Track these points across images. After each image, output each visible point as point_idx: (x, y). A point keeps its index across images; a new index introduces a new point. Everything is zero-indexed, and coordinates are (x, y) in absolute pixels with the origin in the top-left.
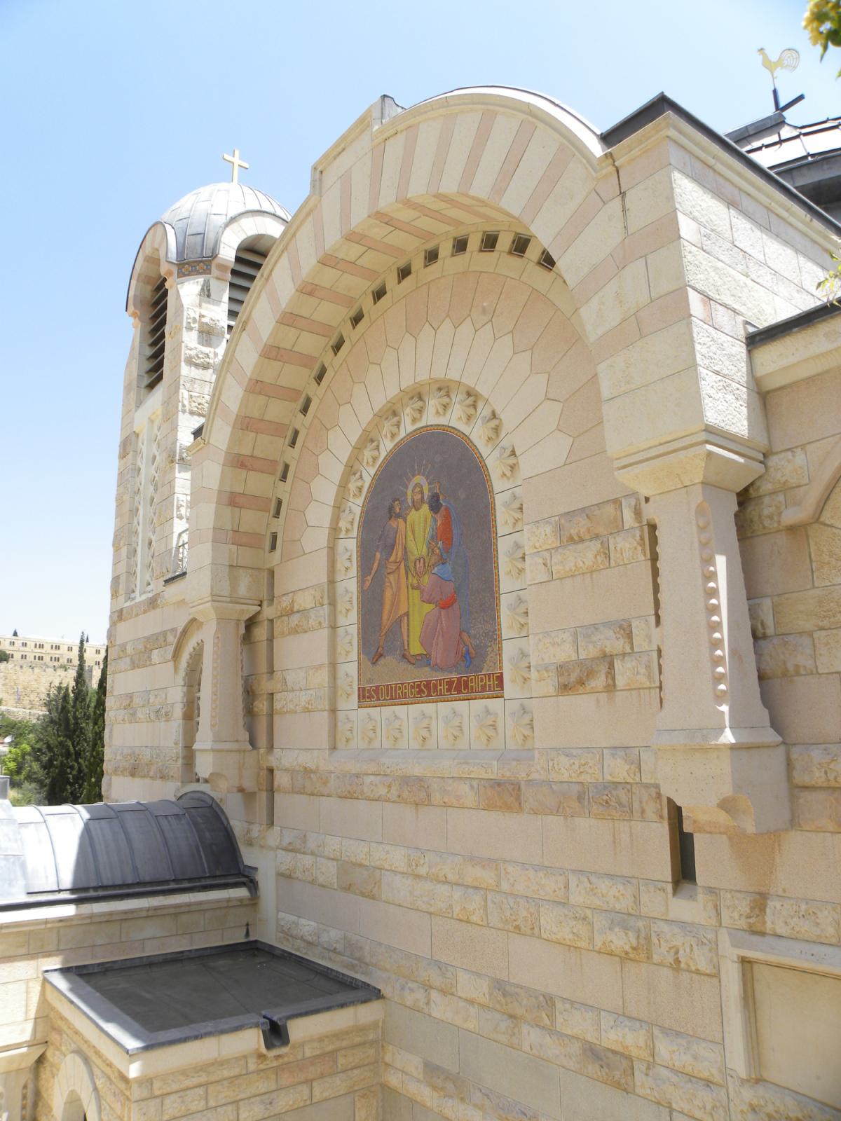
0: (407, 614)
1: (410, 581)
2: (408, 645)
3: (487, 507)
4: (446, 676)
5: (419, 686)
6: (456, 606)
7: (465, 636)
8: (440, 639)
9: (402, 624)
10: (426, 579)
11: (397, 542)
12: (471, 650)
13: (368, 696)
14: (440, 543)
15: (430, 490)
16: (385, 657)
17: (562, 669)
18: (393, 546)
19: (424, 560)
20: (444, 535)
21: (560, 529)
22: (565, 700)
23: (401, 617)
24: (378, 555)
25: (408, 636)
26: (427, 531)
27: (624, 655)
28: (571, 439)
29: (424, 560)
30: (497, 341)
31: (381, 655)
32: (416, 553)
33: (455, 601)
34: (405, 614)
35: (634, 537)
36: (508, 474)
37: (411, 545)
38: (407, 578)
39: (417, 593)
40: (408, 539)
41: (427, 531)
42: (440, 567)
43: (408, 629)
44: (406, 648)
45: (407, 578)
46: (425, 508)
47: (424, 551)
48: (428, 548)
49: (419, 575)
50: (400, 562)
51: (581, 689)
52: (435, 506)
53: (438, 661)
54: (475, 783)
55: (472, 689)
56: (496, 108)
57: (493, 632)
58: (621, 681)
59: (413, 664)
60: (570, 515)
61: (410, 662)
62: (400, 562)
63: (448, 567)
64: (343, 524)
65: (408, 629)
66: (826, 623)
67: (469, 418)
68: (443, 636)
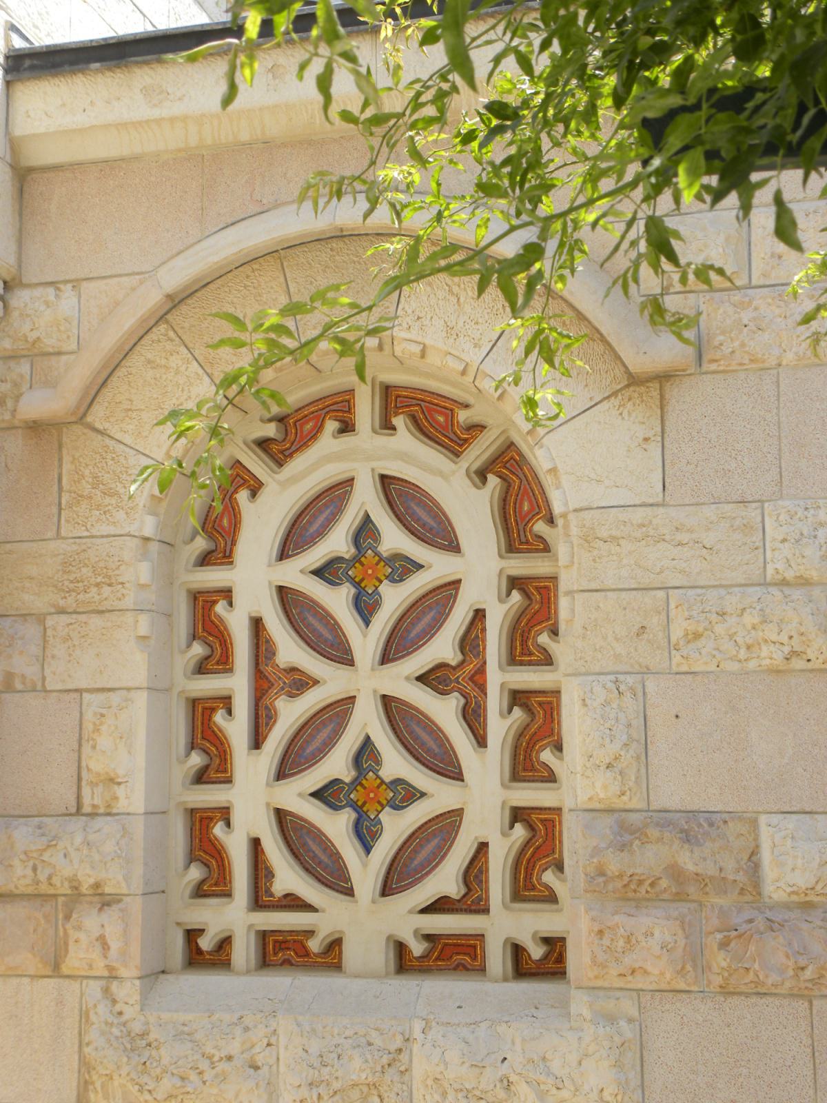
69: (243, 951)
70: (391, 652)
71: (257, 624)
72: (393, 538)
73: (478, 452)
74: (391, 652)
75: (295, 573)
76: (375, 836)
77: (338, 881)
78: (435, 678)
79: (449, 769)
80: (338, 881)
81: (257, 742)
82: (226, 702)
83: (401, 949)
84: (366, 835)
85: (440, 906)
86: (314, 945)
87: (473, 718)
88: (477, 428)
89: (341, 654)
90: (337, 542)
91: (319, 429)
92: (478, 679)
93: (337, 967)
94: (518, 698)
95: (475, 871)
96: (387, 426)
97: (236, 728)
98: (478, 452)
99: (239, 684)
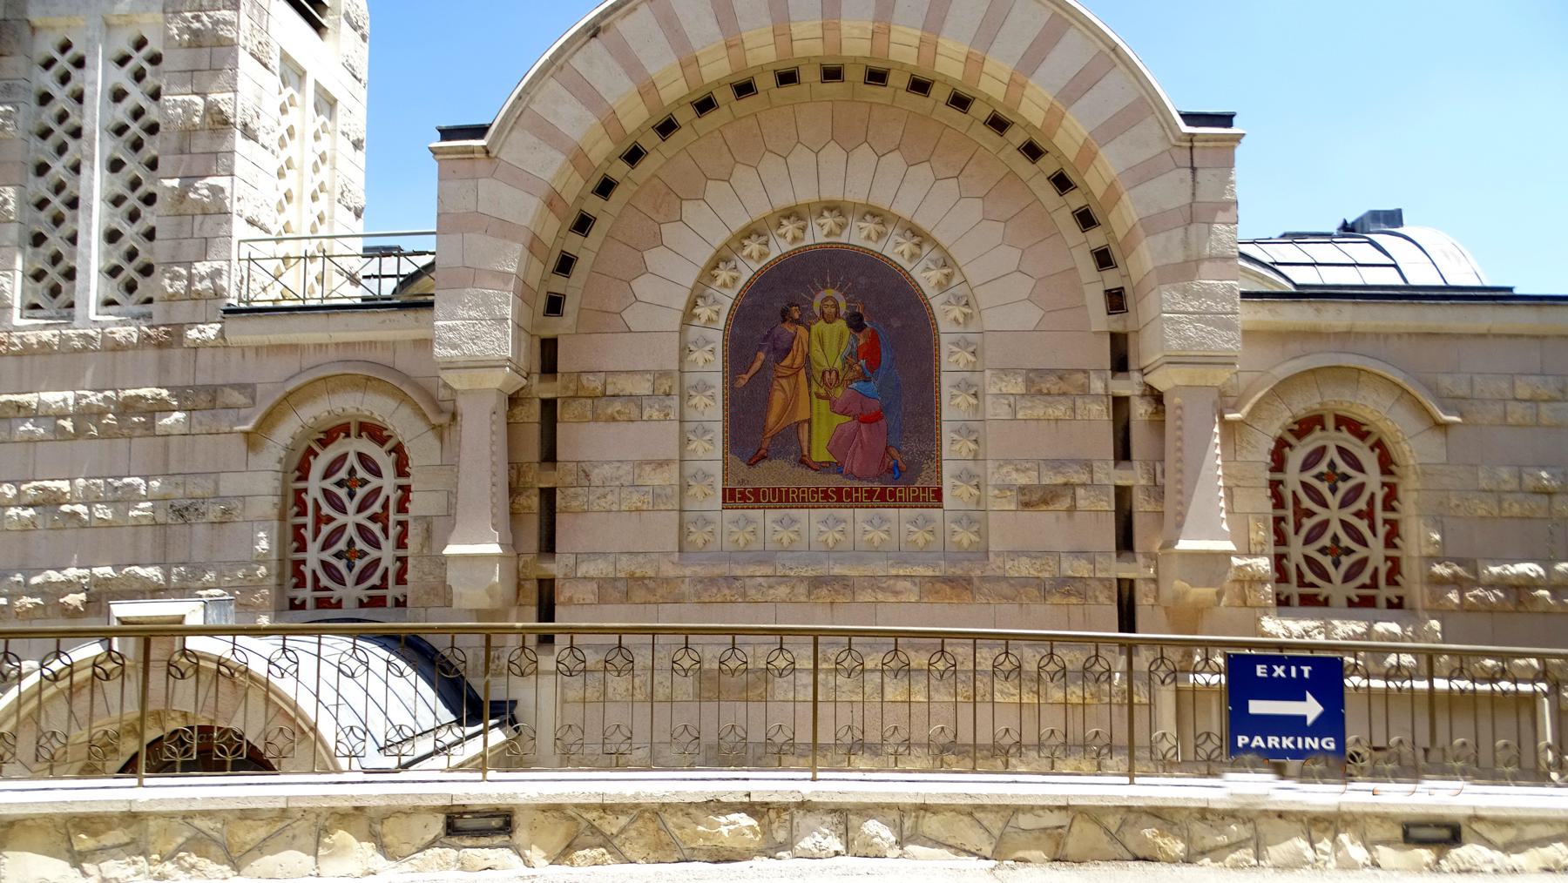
0: (809, 422)
1: (814, 388)
2: (809, 451)
3: (929, 341)
4: (866, 485)
5: (825, 492)
6: (882, 423)
7: (893, 452)
8: (859, 450)
9: (800, 428)
10: (839, 392)
11: (795, 348)
12: (901, 464)
13: (732, 497)
14: (863, 362)
15: (848, 307)
16: (770, 460)
17: (1022, 489)
18: (788, 351)
19: (837, 373)
20: (871, 355)
21: (1029, 382)
22: (1026, 514)
23: (798, 424)
24: (761, 356)
25: (810, 442)
26: (844, 346)
27: (1084, 485)
28: (1043, 312)
29: (837, 373)
30: (962, 200)
31: (764, 457)
32: (825, 364)
33: (882, 418)
34: (805, 421)
35: (1102, 402)
36: (961, 320)
37: (816, 353)
38: (810, 386)
39: (825, 404)
40: (813, 349)
41: (844, 346)
42: (862, 383)
43: (810, 436)
44: (806, 453)
45: (810, 386)
46: (841, 325)
47: (838, 365)
48: (845, 360)
49: (829, 386)
50: (799, 369)
51: (1044, 508)
52: (856, 323)
53: (855, 470)
54: (917, 580)
55: (901, 498)
56: (1072, 20)
57: (931, 452)
58: (1081, 504)
59: (816, 470)
60: (1042, 373)
61: (812, 469)
62: (799, 369)
63: (872, 387)
64: (703, 311)
65: (810, 436)
66: (1241, 483)
67: (913, 256)
68: (862, 447)
69: (310, 604)
70: (360, 510)
71: (316, 501)
72: (361, 473)
73: (389, 445)
74: (360, 510)
75: (329, 484)
76: (353, 567)
77: (341, 582)
78: (373, 518)
79: (377, 545)
80: (341, 582)
81: (315, 540)
82: (304, 526)
83: (361, 601)
84: (350, 567)
85: (374, 587)
86: (333, 601)
87: (385, 530)
88: (390, 437)
89: (343, 510)
90: (342, 474)
91: (338, 436)
92: (387, 518)
93: (340, 607)
94: (400, 523)
95: (384, 577)
96: (360, 436)
97: (308, 534)
98: (389, 445)
99: (309, 520)
